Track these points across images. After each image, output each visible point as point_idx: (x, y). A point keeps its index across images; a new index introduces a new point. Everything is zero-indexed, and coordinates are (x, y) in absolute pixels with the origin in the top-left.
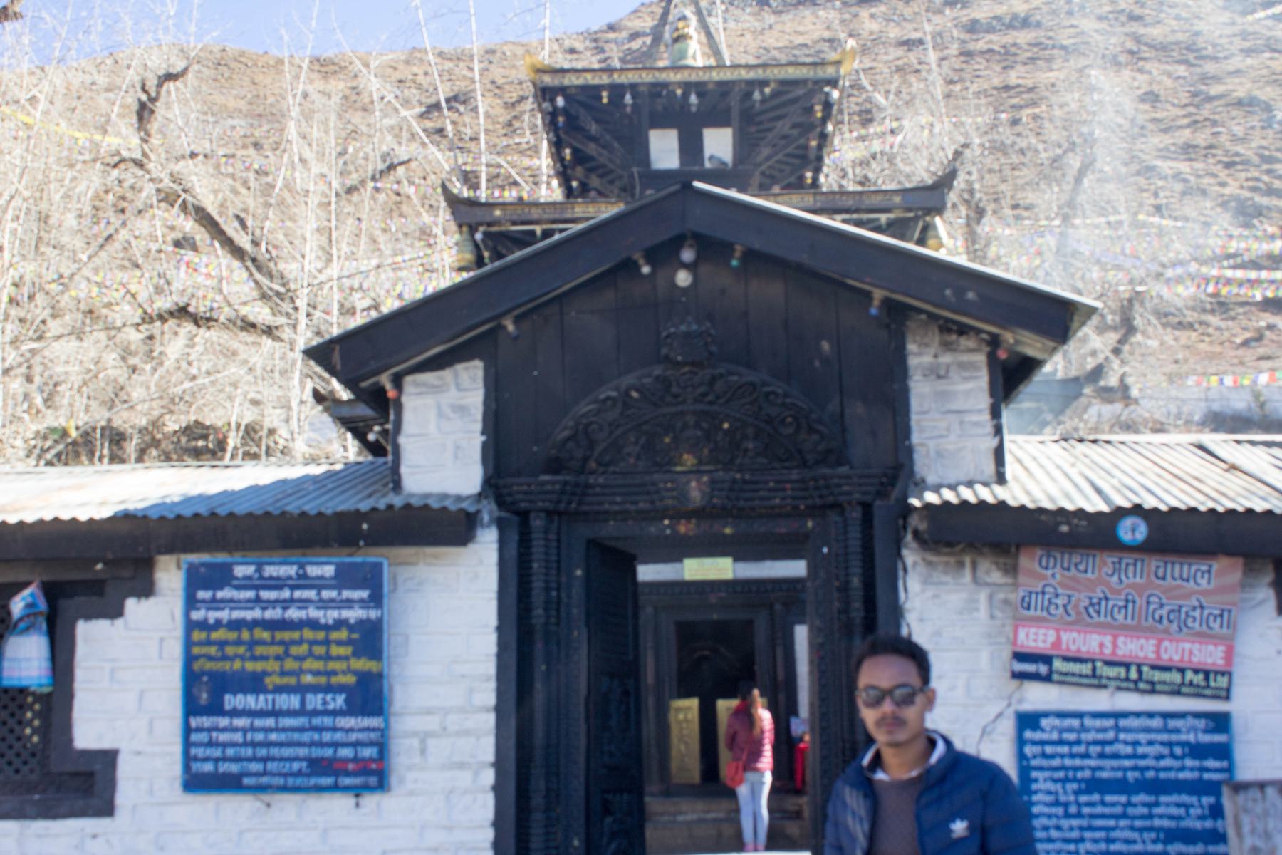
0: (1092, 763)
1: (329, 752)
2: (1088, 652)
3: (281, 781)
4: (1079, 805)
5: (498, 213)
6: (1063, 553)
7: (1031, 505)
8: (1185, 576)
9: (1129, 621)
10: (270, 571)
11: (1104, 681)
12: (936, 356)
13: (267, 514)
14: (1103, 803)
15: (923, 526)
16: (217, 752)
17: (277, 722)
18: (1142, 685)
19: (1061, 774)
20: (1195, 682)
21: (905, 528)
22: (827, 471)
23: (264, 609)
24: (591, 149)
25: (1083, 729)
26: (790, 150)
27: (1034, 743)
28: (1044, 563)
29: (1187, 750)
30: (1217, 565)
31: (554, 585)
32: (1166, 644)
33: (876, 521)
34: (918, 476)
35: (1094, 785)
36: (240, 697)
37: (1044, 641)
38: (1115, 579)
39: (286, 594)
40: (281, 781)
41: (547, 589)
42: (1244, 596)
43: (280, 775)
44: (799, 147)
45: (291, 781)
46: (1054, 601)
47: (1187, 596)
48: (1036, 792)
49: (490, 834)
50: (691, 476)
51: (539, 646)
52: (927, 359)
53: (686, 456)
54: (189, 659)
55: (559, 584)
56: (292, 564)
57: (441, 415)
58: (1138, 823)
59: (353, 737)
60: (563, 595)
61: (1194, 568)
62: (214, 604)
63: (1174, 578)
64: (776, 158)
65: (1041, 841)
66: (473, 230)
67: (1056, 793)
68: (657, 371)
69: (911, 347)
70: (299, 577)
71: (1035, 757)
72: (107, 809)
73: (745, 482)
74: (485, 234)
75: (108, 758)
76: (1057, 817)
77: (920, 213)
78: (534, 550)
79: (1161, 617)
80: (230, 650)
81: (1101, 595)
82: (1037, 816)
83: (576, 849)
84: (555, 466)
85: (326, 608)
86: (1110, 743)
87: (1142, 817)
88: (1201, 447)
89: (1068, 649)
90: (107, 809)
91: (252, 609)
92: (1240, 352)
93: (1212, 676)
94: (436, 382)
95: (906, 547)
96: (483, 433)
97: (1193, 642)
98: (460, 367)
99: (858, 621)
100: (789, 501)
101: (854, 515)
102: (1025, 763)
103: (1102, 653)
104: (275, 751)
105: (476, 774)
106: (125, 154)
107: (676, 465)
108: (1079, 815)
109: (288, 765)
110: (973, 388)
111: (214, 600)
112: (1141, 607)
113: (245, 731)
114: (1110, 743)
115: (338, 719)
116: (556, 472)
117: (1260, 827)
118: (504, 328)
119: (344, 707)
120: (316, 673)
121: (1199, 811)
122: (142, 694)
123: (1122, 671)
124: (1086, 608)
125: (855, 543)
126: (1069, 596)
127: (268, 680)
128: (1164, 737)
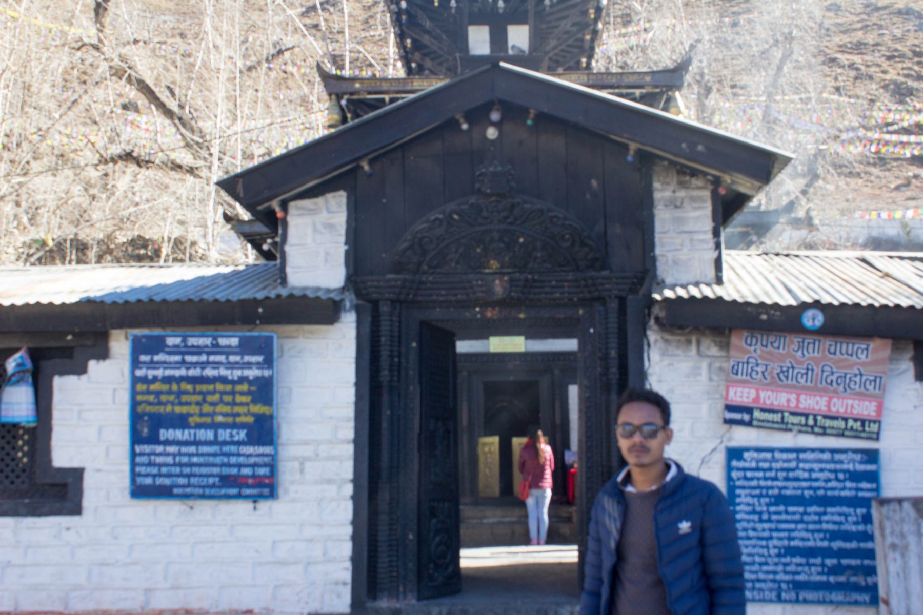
0: (780, 484)
1: (234, 471)
2: (779, 406)
3: (200, 491)
4: (769, 513)
5: (357, 85)
6: (762, 335)
7: (740, 300)
8: (850, 352)
9: (809, 384)
10: (192, 341)
11: (789, 426)
12: (674, 192)
13: (190, 300)
14: (787, 512)
15: (662, 314)
16: (155, 470)
17: (197, 450)
18: (816, 430)
19: (757, 492)
20: (855, 428)
21: (649, 315)
22: (593, 273)
23: (188, 369)
24: (426, 39)
25: (774, 460)
26: (570, 42)
27: (739, 469)
28: (749, 342)
29: (847, 475)
30: (874, 344)
31: (396, 353)
32: (835, 400)
33: (629, 311)
34: (660, 278)
35: (782, 500)
36: (171, 431)
37: (748, 397)
38: (800, 353)
39: (204, 358)
40: (200, 491)
41: (391, 357)
42: (892, 367)
43: (200, 487)
44: (576, 40)
45: (207, 491)
46: (755, 368)
47: (851, 366)
48: (739, 504)
49: (349, 530)
50: (497, 276)
51: (385, 398)
52: (668, 194)
53: (492, 262)
54: (134, 404)
55: (400, 352)
56: (208, 336)
57: (315, 230)
58: (811, 527)
59: (252, 460)
60: (403, 360)
61: (856, 346)
62: (152, 365)
63: (842, 354)
64: (560, 48)
65: (742, 538)
66: (339, 97)
67: (754, 505)
68: (472, 200)
69: (656, 185)
70: (213, 346)
71: (739, 479)
72: (76, 509)
73: (535, 281)
74: (348, 100)
75: (77, 474)
76: (754, 521)
77: (664, 89)
78: (382, 328)
79: (832, 381)
80: (164, 398)
81: (789, 365)
82: (740, 521)
83: (411, 541)
84: (398, 268)
85: (232, 368)
86: (793, 470)
87: (814, 522)
88: (864, 261)
89: (765, 403)
90: (76, 509)
91: (179, 368)
92: (894, 194)
93: (867, 424)
94: (312, 207)
95: (650, 329)
96: (346, 244)
97: (854, 399)
98: (329, 196)
99: (614, 381)
100: (566, 295)
101: (613, 305)
102: (732, 483)
103: (788, 406)
104: (196, 470)
105: (340, 487)
106: (86, 40)
107: (485, 268)
108: (769, 521)
109: (205, 480)
110: (701, 216)
111: (152, 362)
112: (817, 374)
113: (174, 455)
114: (793, 470)
115: (241, 448)
116: (398, 272)
117: (897, 529)
118: (362, 167)
119: (246, 439)
120: (225, 415)
121: (855, 519)
122: (100, 429)
123: (803, 419)
124: (778, 374)
125: (613, 326)
126: (766, 366)
127: (191, 420)
128: (831, 466)
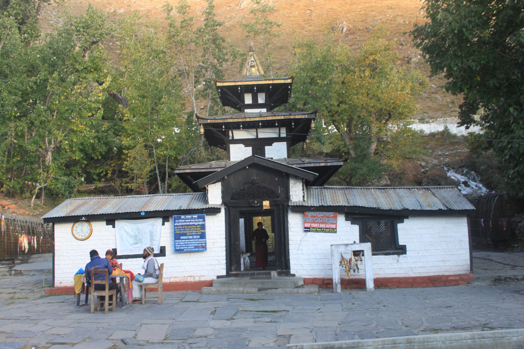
10: (187, 217)
54: (175, 231)
62: (178, 222)
